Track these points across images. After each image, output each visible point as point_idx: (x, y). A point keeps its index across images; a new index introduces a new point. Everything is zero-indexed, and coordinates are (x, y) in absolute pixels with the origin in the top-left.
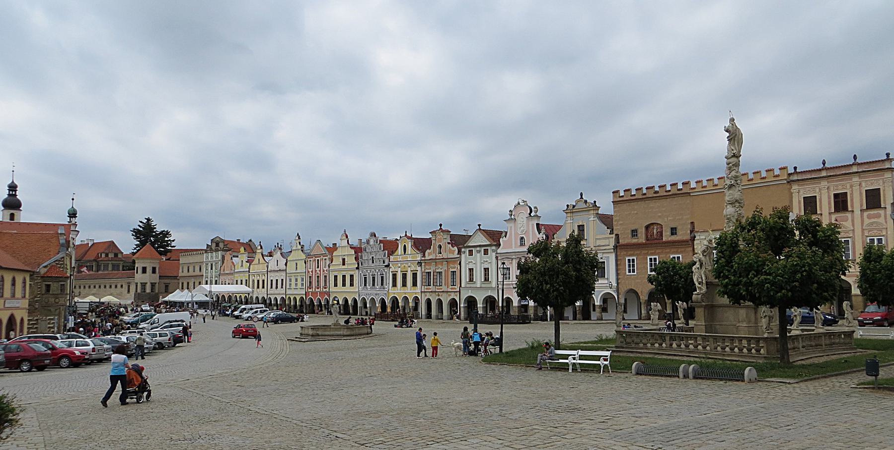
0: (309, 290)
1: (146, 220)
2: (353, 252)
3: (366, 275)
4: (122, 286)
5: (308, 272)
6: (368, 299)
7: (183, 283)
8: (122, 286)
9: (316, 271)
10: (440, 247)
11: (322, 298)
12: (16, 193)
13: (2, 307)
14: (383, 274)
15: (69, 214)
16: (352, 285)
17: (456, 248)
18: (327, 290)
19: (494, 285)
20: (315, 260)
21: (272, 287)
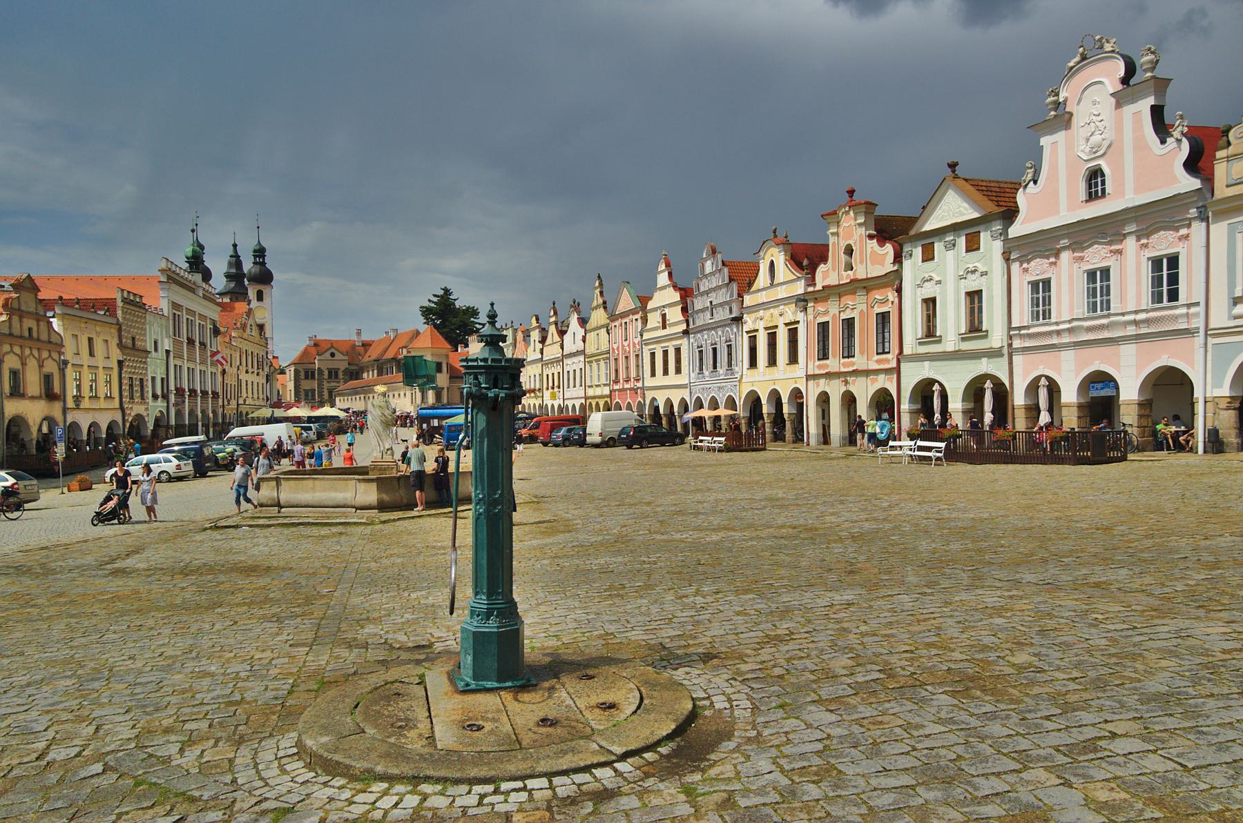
0: (616, 387)
2: (677, 297)
3: (702, 347)
4: (405, 394)
5: (613, 349)
6: (706, 401)
8: (405, 394)
9: (623, 346)
10: (849, 251)
11: (634, 402)
12: (264, 259)
14: (730, 341)
15: (187, 258)
16: (678, 371)
17: (889, 249)
18: (640, 385)
19: (997, 339)
20: (621, 325)
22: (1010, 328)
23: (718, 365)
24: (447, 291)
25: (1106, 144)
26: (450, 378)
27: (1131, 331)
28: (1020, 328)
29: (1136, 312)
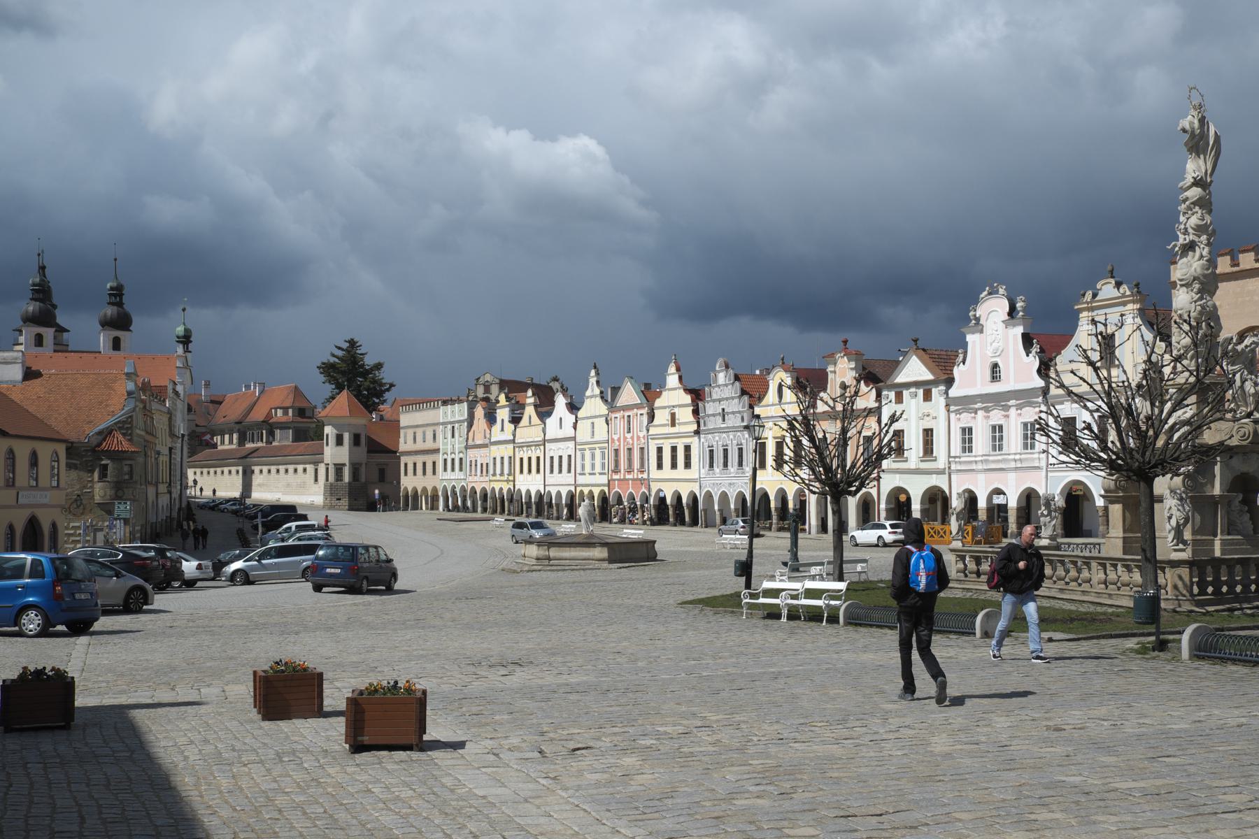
0: (616, 477)
1: (348, 344)
2: (687, 399)
4: (305, 470)
5: (613, 439)
6: (716, 494)
7: (406, 465)
8: (305, 470)
9: (625, 438)
11: (637, 493)
12: (121, 299)
13: (14, 503)
14: (741, 444)
18: (645, 476)
19: (941, 463)
20: (624, 417)
21: (552, 471)
22: (949, 456)
23: (729, 464)
24: (352, 343)
25: (1001, 349)
26: (369, 451)
27: (1013, 465)
28: (955, 457)
29: (1015, 454)
